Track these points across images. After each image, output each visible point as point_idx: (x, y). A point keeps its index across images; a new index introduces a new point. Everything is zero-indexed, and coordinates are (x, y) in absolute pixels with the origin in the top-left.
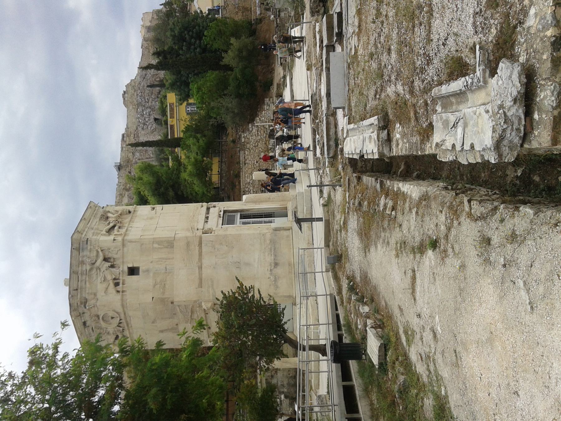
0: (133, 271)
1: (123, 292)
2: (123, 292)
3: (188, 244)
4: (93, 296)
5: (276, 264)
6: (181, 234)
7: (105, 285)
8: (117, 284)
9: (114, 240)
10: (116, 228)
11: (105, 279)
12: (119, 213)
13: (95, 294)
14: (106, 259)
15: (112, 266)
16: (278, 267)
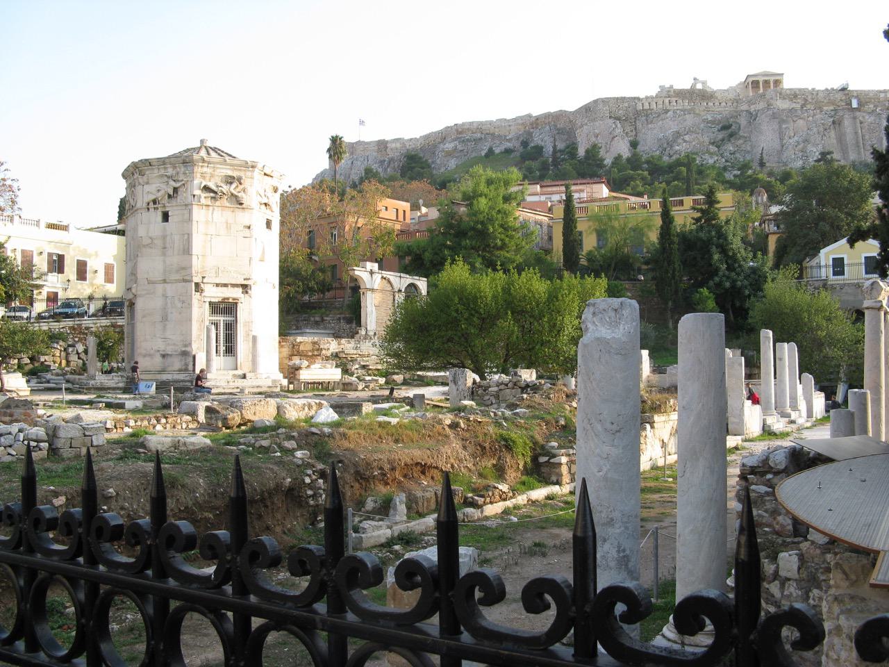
0: (166, 217)
1: (148, 209)
2: (148, 209)
3: (184, 268)
4: (146, 181)
5: (164, 356)
6: (196, 264)
7: (155, 192)
8: (154, 202)
9: (194, 196)
10: (212, 195)
11: (159, 191)
12: (239, 195)
13: (147, 183)
14: (175, 190)
15: (170, 196)
16: (161, 359)
